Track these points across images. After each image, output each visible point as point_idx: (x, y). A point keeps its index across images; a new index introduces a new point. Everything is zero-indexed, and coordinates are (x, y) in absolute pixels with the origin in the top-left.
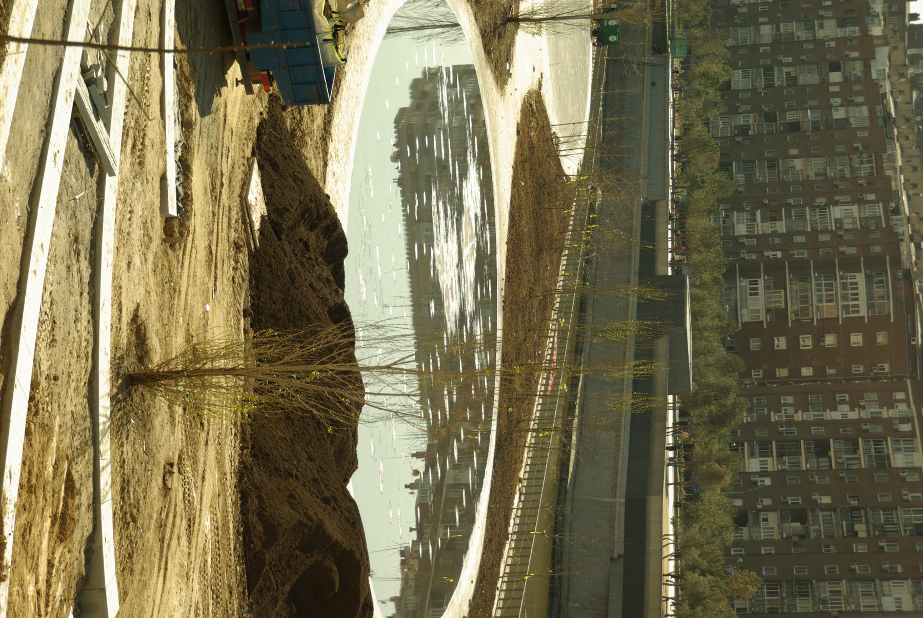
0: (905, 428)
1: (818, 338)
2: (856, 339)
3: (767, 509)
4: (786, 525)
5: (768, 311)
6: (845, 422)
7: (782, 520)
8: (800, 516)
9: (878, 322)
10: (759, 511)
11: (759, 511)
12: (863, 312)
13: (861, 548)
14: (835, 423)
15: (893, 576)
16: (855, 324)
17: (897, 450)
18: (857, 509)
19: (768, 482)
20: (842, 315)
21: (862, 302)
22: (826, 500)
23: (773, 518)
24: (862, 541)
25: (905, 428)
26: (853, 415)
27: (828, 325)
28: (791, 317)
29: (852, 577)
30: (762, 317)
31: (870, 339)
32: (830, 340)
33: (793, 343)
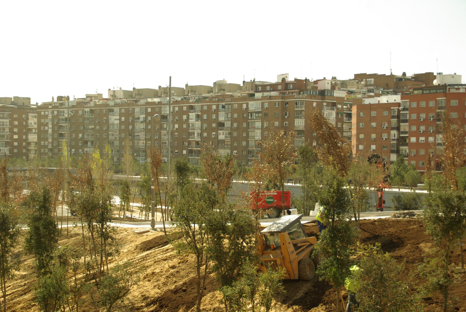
0: (56, 113)
1: (15, 133)
2: (16, 123)
3: (83, 151)
4: (89, 146)
5: (6, 147)
6: (53, 128)
7: (87, 147)
8: (86, 142)
9: (11, 117)
10: (84, 153)
11: (84, 153)
12: (8, 120)
13: (98, 127)
14: (53, 131)
15: (107, 121)
16: (11, 123)
17: (63, 115)
18: (84, 127)
19: (73, 150)
20: (8, 126)
21: (5, 120)
22: (80, 135)
23: (86, 149)
24: (95, 127)
25: (56, 113)
26: (50, 126)
27: (11, 131)
28: (8, 140)
29: (108, 130)
30: (8, 148)
31: (16, 119)
32: (16, 130)
33: (16, 140)
